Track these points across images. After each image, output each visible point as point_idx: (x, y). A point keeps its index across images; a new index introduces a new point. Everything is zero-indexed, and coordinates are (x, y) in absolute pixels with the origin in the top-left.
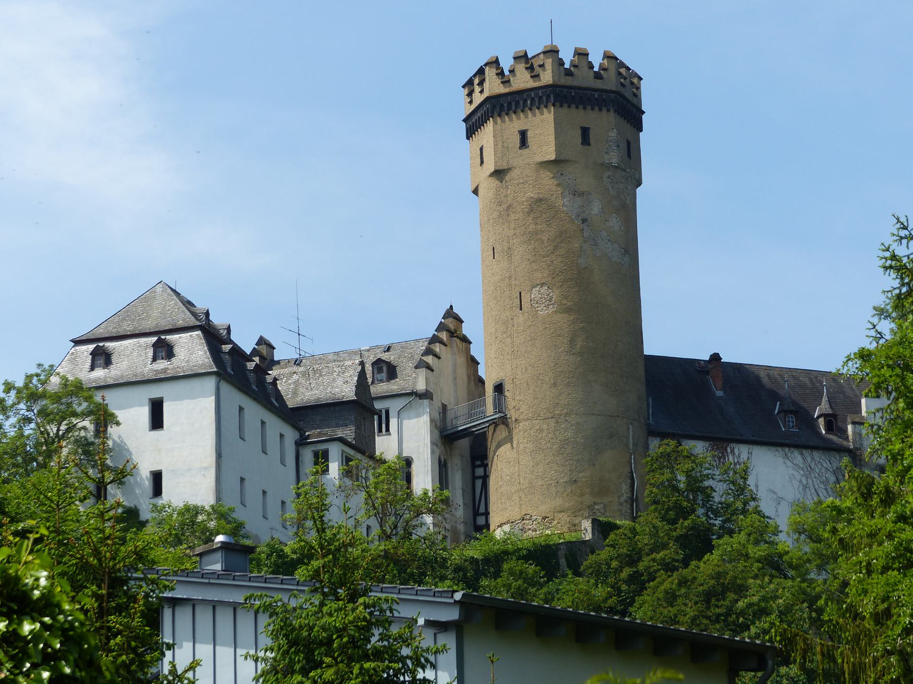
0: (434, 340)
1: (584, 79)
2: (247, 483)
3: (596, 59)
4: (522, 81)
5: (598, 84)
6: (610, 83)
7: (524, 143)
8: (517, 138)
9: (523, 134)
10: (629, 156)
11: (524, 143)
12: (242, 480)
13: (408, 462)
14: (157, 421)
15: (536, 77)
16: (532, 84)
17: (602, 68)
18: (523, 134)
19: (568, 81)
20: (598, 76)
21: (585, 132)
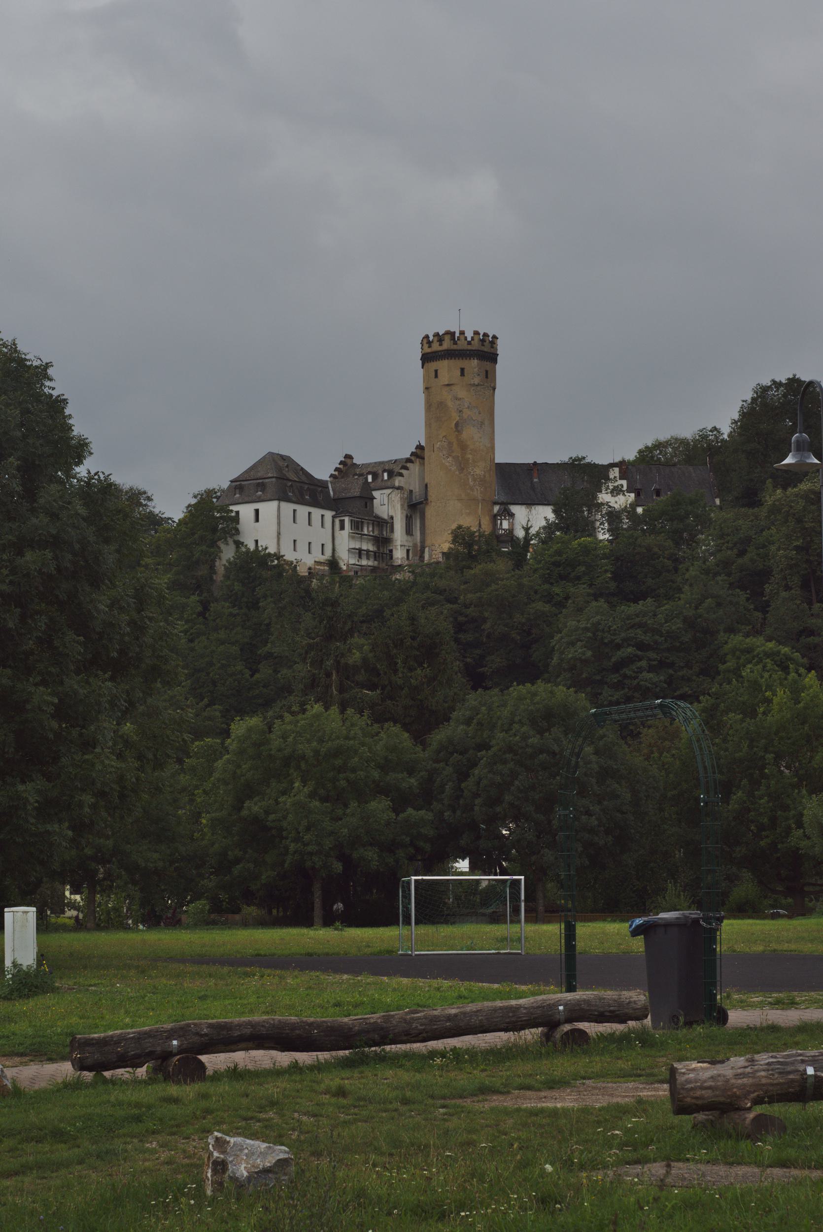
0: (408, 460)
1: (462, 345)
2: (297, 543)
3: (469, 335)
4: (436, 347)
5: (469, 347)
6: (476, 345)
7: (436, 376)
8: (433, 374)
9: (436, 371)
10: (487, 377)
11: (436, 376)
12: (295, 541)
13: (392, 518)
14: (257, 520)
15: (441, 345)
16: (440, 348)
17: (473, 338)
18: (436, 371)
19: (455, 347)
20: (469, 343)
21: (462, 370)
